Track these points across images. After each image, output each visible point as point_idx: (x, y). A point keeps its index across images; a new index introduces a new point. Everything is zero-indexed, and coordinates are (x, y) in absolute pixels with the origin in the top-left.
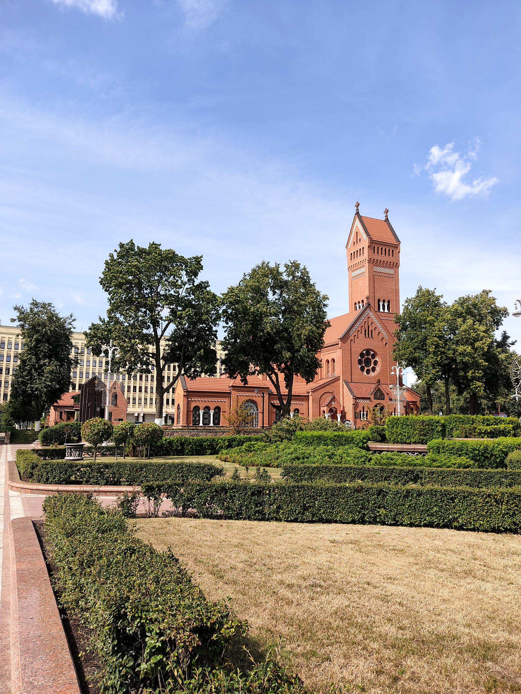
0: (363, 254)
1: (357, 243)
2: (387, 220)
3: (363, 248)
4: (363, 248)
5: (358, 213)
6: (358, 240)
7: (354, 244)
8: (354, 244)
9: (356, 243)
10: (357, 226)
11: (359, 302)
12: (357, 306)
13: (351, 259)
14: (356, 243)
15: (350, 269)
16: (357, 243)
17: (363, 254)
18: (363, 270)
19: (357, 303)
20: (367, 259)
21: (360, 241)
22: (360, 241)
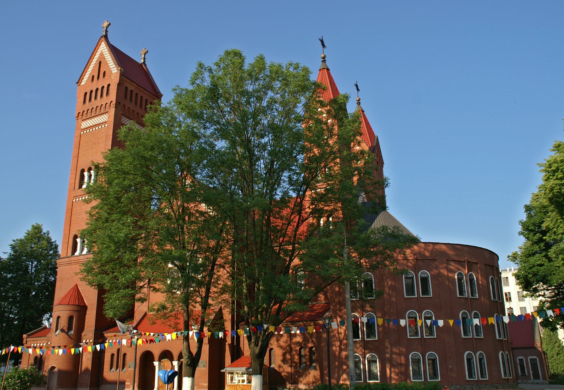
0: (107, 94)
1: (98, 78)
2: (144, 63)
3: (109, 85)
4: (109, 85)
5: (106, 37)
6: (101, 75)
7: (93, 80)
8: (93, 80)
9: (96, 78)
10: (102, 54)
11: (90, 169)
12: (86, 174)
13: (84, 102)
14: (96, 78)
15: (80, 117)
16: (98, 78)
17: (107, 94)
18: (104, 118)
19: (86, 169)
20: (114, 102)
21: (104, 75)
22: (104, 75)
